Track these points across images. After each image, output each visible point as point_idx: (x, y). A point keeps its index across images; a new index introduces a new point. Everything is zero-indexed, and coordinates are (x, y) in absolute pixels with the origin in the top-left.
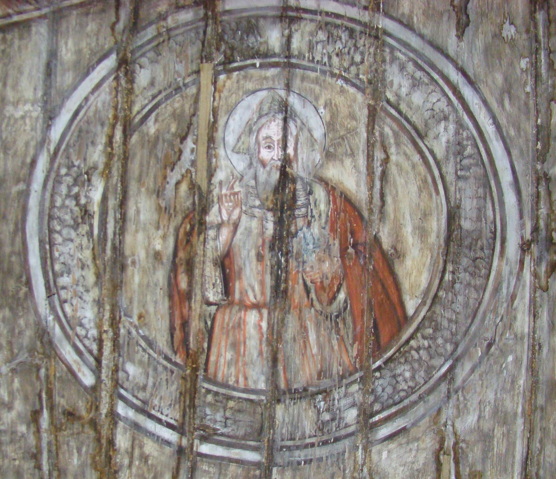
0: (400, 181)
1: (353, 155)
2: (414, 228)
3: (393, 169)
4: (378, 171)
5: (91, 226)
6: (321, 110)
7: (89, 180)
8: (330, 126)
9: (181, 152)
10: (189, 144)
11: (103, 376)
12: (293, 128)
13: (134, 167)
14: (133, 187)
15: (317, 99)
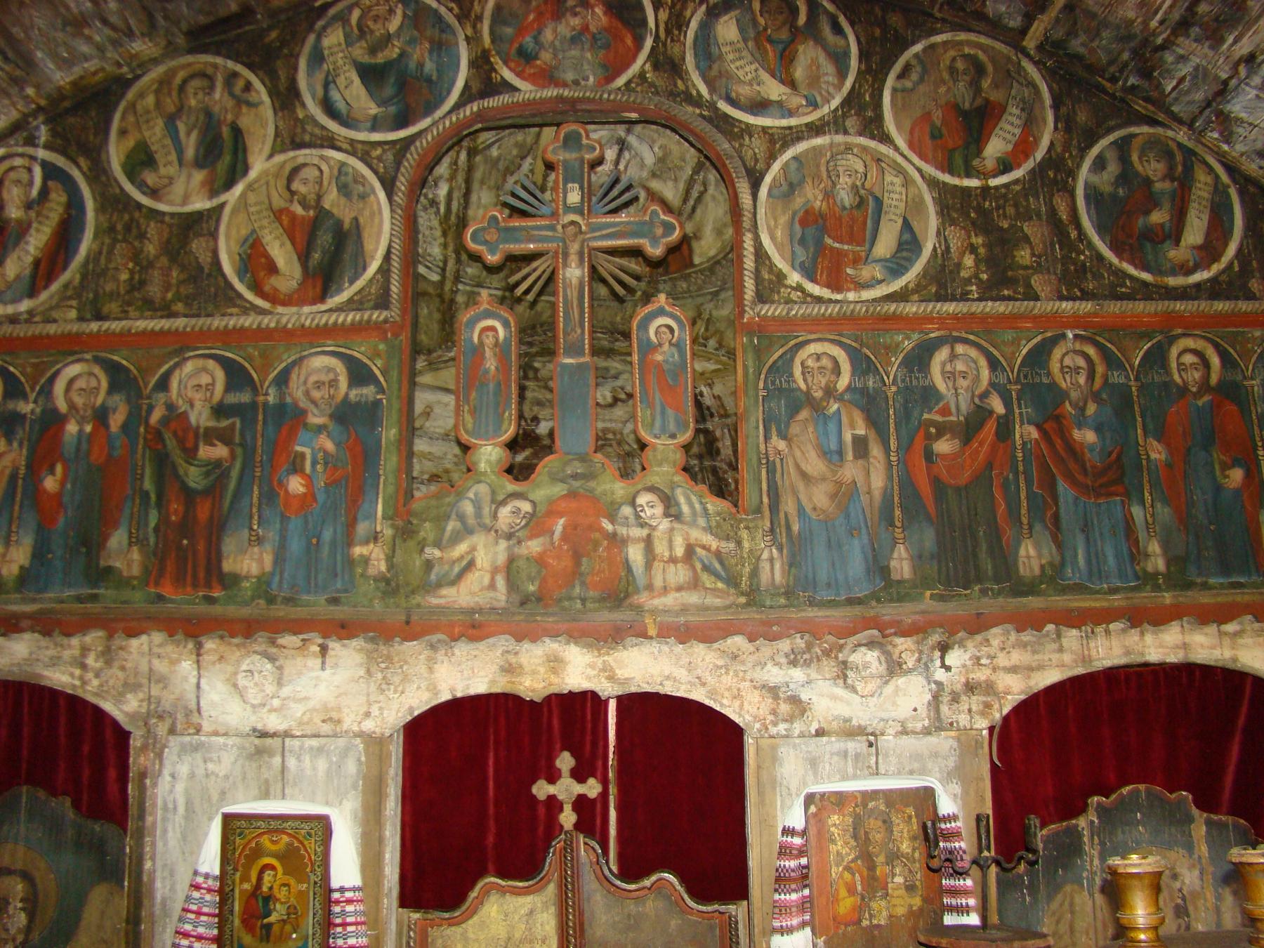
0: (711, 205)
1: (676, 180)
2: (714, 229)
3: (707, 197)
4: (695, 194)
5: (438, 209)
6: (656, 149)
7: (436, 185)
8: (661, 160)
9: (520, 166)
10: (529, 160)
11: (448, 274)
12: (626, 155)
13: (478, 175)
14: (476, 186)
15: (654, 141)
